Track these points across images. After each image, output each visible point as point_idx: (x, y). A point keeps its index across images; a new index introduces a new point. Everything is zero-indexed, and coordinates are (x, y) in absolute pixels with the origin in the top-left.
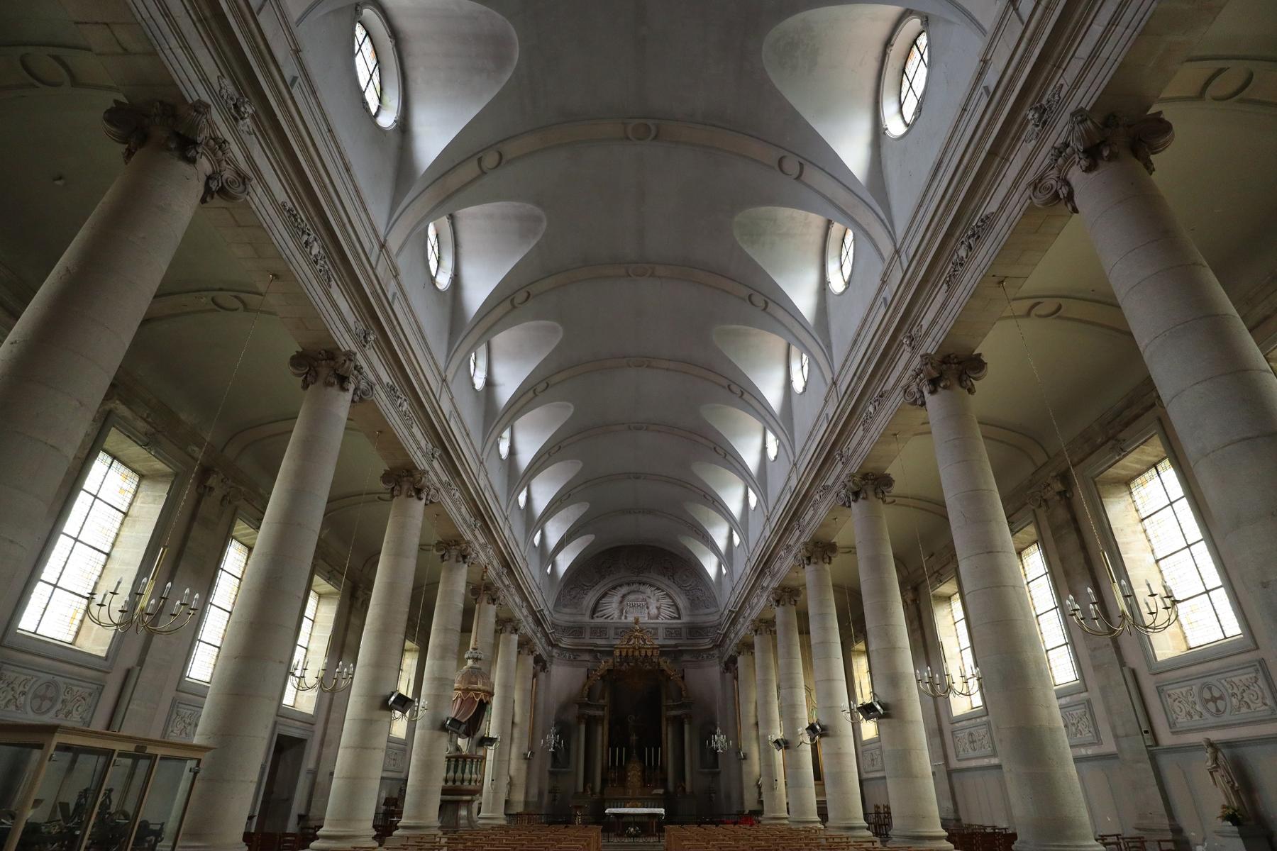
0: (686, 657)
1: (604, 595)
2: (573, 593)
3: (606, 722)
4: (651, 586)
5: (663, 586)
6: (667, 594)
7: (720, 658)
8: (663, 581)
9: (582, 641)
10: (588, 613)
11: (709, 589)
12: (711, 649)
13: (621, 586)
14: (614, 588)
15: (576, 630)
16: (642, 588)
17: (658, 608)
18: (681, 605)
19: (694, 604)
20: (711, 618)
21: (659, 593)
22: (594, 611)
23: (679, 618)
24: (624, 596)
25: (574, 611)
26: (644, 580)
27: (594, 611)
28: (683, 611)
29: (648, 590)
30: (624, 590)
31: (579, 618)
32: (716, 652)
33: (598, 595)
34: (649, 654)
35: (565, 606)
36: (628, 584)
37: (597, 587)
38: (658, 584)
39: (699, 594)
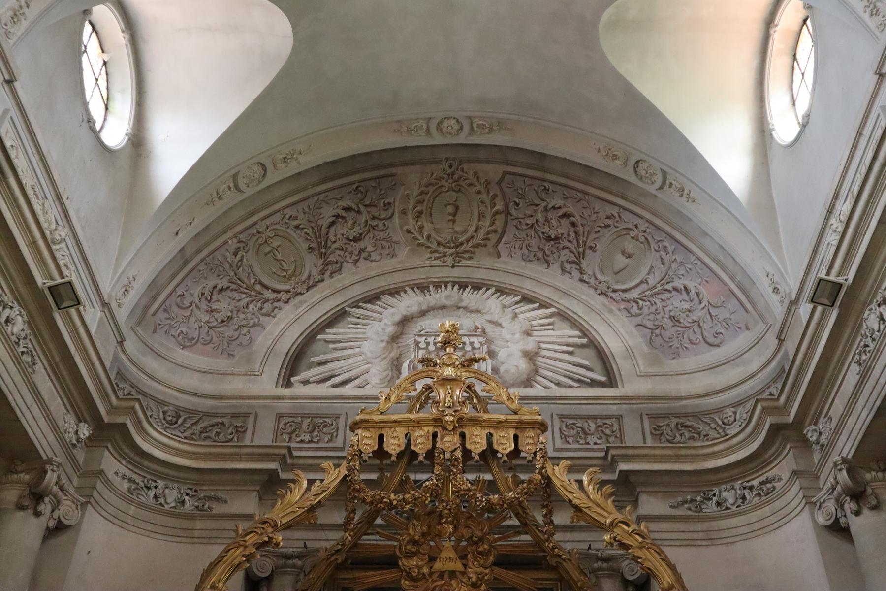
0: (650, 505)
1: (337, 317)
2: (224, 306)
4: (501, 291)
5: (545, 293)
6: (563, 316)
7: (806, 475)
8: (548, 281)
10: (274, 368)
11: (725, 232)
12: (756, 461)
13: (395, 292)
14: (373, 298)
15: (221, 423)
16: (469, 298)
17: (531, 356)
18: (612, 343)
19: (664, 338)
20: (733, 374)
21: (529, 314)
22: (295, 363)
23: (611, 382)
24: (405, 321)
25: (222, 363)
26: (479, 275)
27: (295, 363)
28: (622, 365)
29: (492, 304)
30: (409, 302)
31: (236, 385)
32: (783, 468)
33: (312, 318)
34: (504, 444)
35: (188, 342)
36: (423, 288)
37: (314, 296)
38: (528, 286)
39: (678, 303)
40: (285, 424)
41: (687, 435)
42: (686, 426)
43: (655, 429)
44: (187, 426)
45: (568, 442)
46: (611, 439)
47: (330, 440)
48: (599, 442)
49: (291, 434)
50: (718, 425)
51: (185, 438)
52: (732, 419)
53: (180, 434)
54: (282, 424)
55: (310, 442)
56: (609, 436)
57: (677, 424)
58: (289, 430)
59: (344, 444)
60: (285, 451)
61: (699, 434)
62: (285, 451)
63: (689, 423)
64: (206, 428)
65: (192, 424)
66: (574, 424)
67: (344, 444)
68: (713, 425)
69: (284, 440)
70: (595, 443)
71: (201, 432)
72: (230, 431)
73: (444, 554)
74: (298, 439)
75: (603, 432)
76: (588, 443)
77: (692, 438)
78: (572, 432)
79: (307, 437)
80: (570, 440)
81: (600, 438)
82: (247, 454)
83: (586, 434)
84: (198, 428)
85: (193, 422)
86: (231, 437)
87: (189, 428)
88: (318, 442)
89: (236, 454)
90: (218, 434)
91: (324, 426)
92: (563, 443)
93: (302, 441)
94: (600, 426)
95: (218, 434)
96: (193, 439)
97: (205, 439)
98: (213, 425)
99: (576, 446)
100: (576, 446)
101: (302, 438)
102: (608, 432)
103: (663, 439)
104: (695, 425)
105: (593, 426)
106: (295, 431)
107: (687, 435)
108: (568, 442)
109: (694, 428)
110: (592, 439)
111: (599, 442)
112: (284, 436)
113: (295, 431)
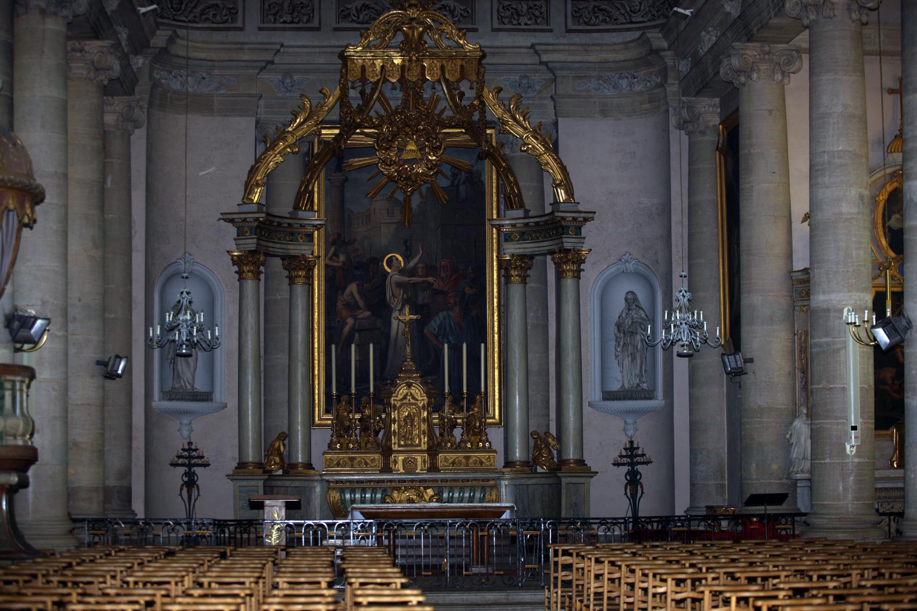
3: (318, 274)
9: (233, 36)
40: (269, 6)
41: (601, 18)
42: (602, 10)
43: (576, 12)
44: (190, 9)
45: (503, 23)
46: (539, 20)
47: (308, 21)
48: (529, 22)
49: (275, 15)
50: (627, 12)
51: (190, 21)
52: (638, 8)
53: (185, 19)
54: (266, 6)
55: (292, 22)
56: (537, 17)
57: (595, 7)
58: (273, 11)
59: (320, 24)
60: (278, 47)
61: (610, 17)
62: (278, 47)
63: (604, 7)
64: (204, 10)
65: (193, 8)
66: (510, 5)
67: (320, 24)
68: (623, 11)
69: (270, 22)
70: (526, 24)
71: (201, 15)
72: (224, 13)
73: (410, 147)
74: (282, 20)
75: (533, 14)
76: (520, 24)
77: (604, 21)
78: (508, 13)
79: (289, 19)
80: (506, 21)
81: (530, 19)
82: (250, 49)
83: (519, 15)
84: (197, 11)
85: (193, 5)
86: (225, 18)
87: (191, 12)
88: (297, 23)
89: (241, 49)
90: (215, 15)
91: (302, 7)
92: (499, 24)
93: (285, 22)
94: (531, 8)
95: (215, 15)
96: (196, 22)
97: (206, 20)
98: (209, 7)
99: (510, 26)
100: (510, 26)
101: (285, 18)
102: (537, 13)
103: (581, 21)
104: (609, 9)
105: (525, 7)
106: (278, 12)
107: (601, 18)
108: (503, 23)
109: (608, 12)
110: (523, 20)
111: (529, 22)
112: (270, 17)
113: (278, 12)
